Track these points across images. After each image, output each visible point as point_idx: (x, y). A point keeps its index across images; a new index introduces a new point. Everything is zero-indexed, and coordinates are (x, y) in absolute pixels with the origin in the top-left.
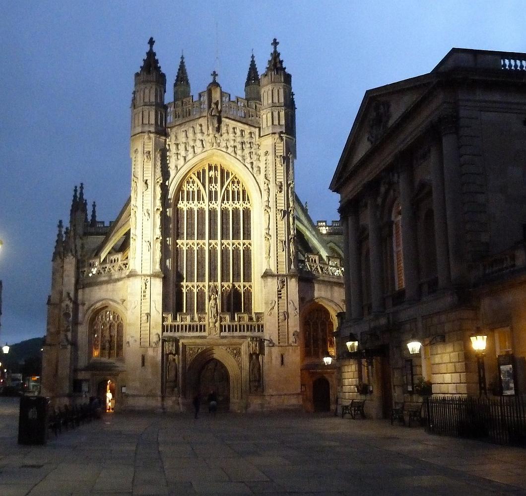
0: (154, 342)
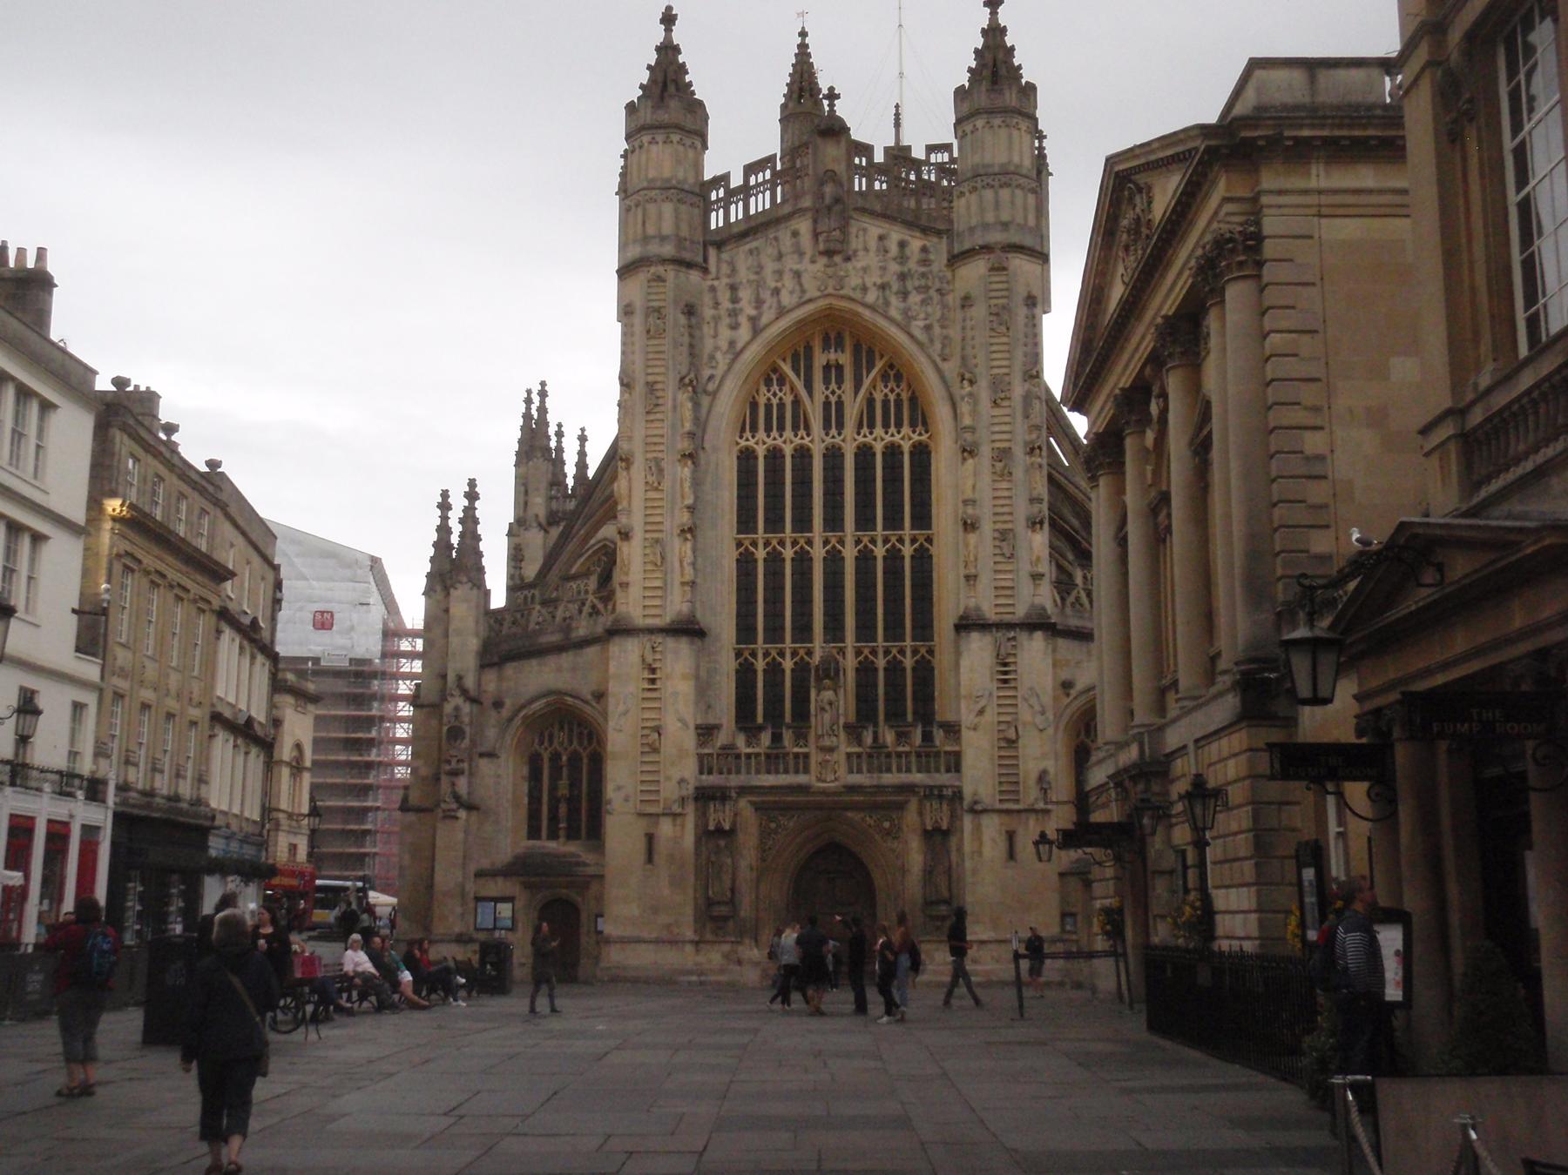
0: (675, 802)
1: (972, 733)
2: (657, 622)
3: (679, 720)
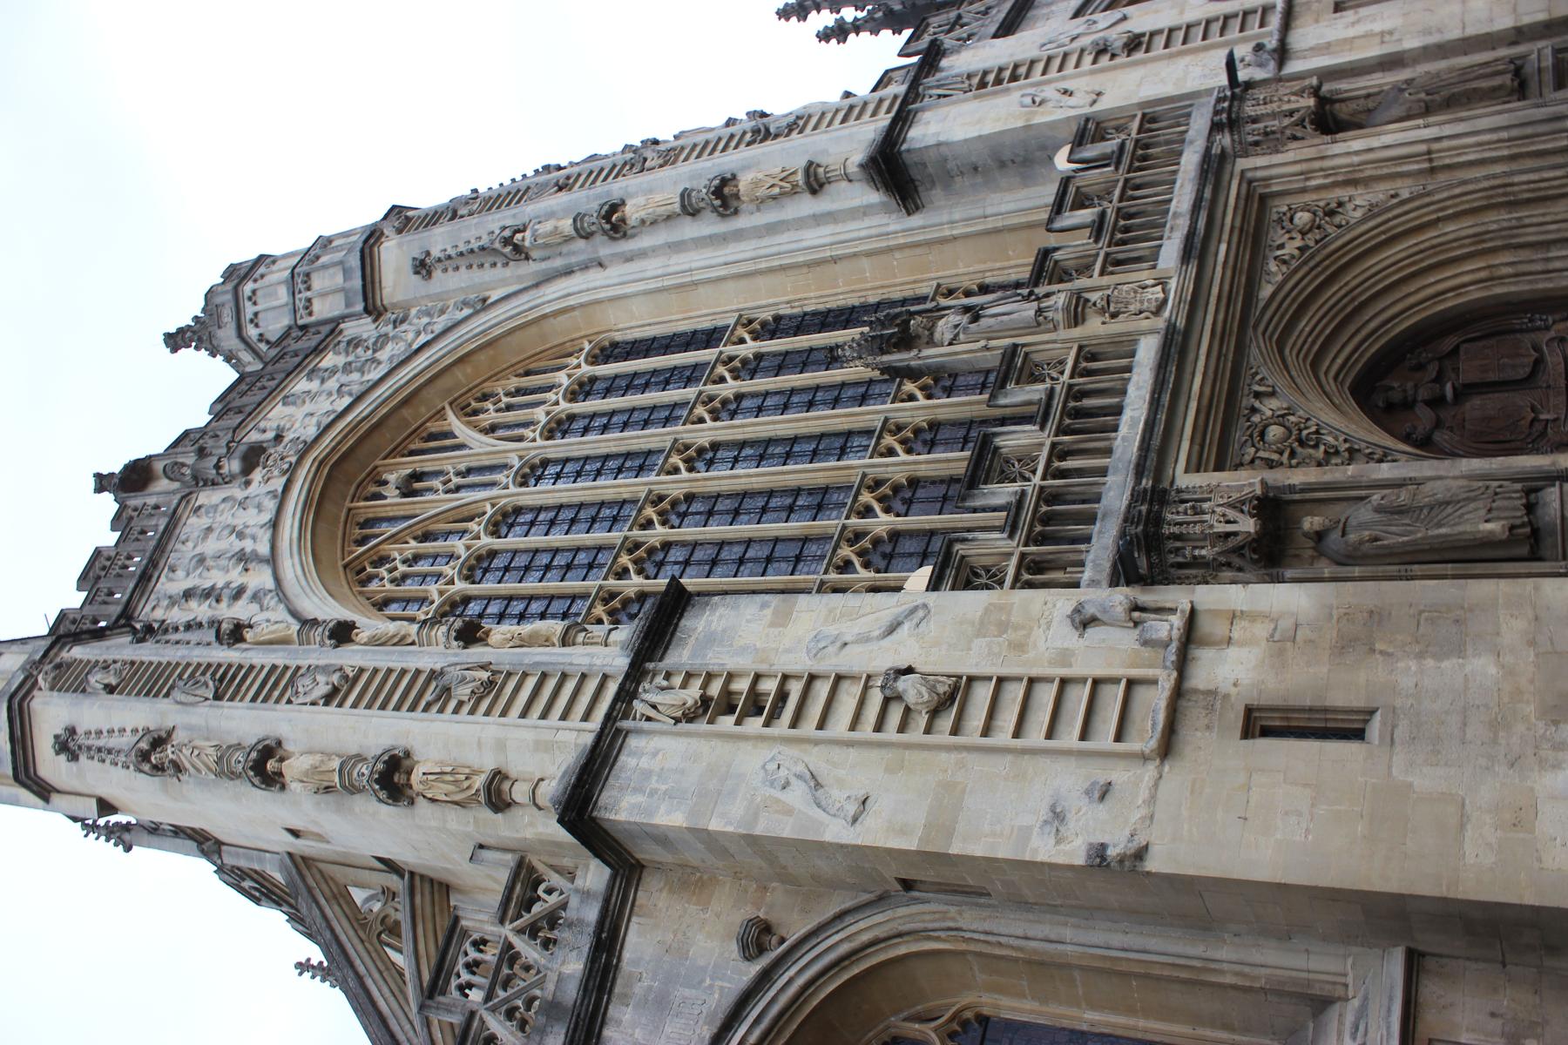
1: (1103, 98)
2: (612, 688)
3: (892, 629)
